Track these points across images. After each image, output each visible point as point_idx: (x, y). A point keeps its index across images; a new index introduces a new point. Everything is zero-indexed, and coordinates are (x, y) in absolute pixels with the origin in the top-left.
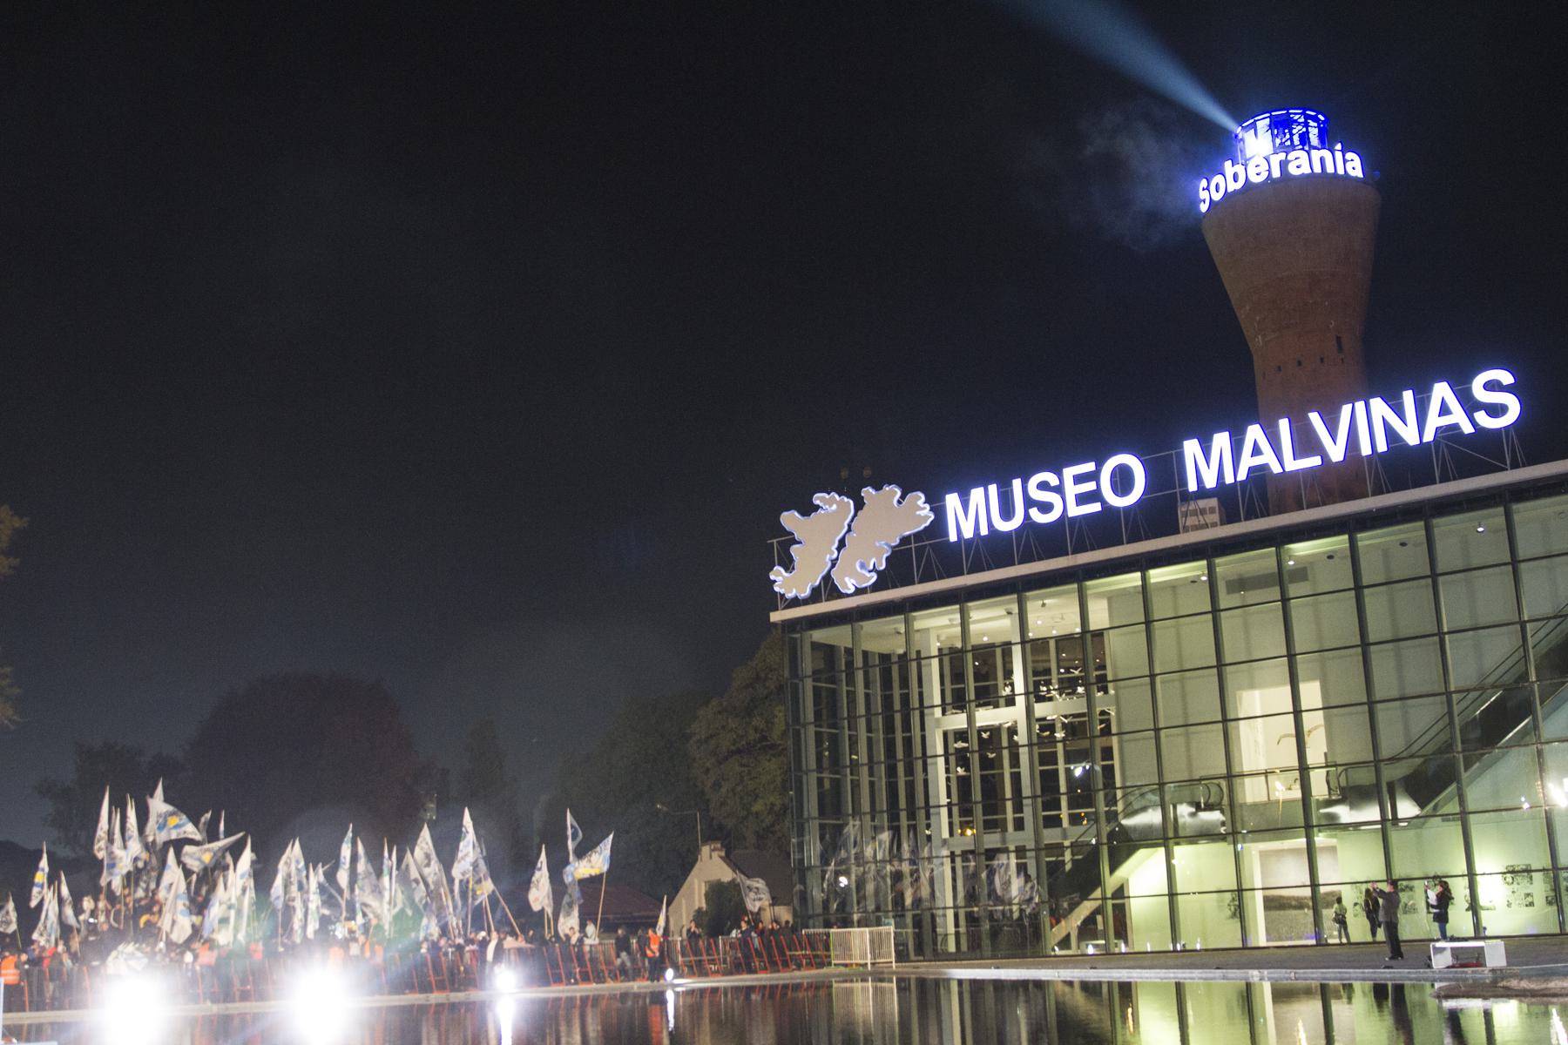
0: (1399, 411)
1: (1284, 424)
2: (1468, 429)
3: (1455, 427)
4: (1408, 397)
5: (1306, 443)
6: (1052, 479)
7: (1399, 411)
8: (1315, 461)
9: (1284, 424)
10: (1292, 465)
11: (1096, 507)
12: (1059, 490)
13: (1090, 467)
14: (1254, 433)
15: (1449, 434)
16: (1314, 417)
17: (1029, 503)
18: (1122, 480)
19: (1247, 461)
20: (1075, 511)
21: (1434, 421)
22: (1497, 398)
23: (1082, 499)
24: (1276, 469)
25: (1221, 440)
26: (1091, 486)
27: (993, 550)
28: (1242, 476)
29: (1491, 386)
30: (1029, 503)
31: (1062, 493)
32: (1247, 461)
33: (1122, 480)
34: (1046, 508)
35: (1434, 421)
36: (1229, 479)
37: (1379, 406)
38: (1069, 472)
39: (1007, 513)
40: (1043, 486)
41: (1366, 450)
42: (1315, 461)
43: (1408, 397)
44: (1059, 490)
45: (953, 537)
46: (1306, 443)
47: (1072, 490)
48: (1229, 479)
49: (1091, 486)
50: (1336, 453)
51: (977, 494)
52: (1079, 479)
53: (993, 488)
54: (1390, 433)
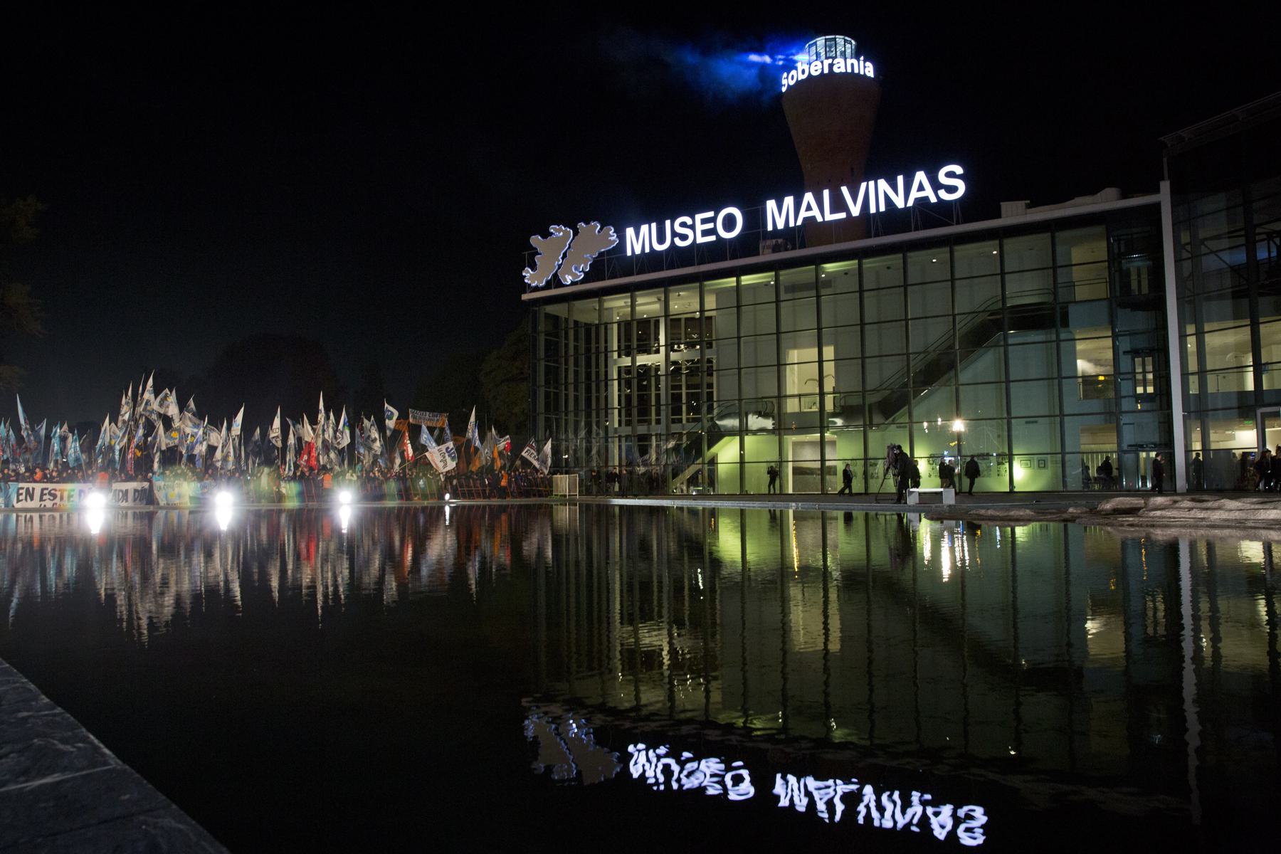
0: (894, 187)
1: (826, 193)
2: (933, 200)
3: (927, 198)
4: (900, 179)
5: (838, 204)
6: (688, 220)
7: (894, 187)
8: (843, 215)
9: (826, 193)
10: (829, 217)
11: (713, 238)
12: (693, 227)
13: (711, 214)
14: (809, 197)
15: (922, 202)
16: (844, 190)
17: (674, 234)
18: (729, 223)
19: (803, 214)
20: (701, 240)
21: (914, 194)
22: (952, 182)
23: (705, 233)
24: (820, 219)
25: (789, 201)
26: (711, 226)
27: (651, 260)
28: (799, 222)
29: (951, 175)
30: (674, 234)
31: (693, 229)
32: (803, 214)
33: (729, 223)
34: (684, 237)
35: (914, 194)
36: (792, 224)
37: (883, 184)
38: (699, 217)
39: (661, 239)
40: (683, 225)
41: (873, 210)
42: (843, 215)
43: (900, 179)
44: (693, 227)
45: (629, 253)
46: (838, 204)
47: (700, 228)
48: (792, 224)
49: (711, 226)
50: (855, 211)
51: (644, 228)
52: (704, 221)
53: (654, 225)
54: (888, 201)
